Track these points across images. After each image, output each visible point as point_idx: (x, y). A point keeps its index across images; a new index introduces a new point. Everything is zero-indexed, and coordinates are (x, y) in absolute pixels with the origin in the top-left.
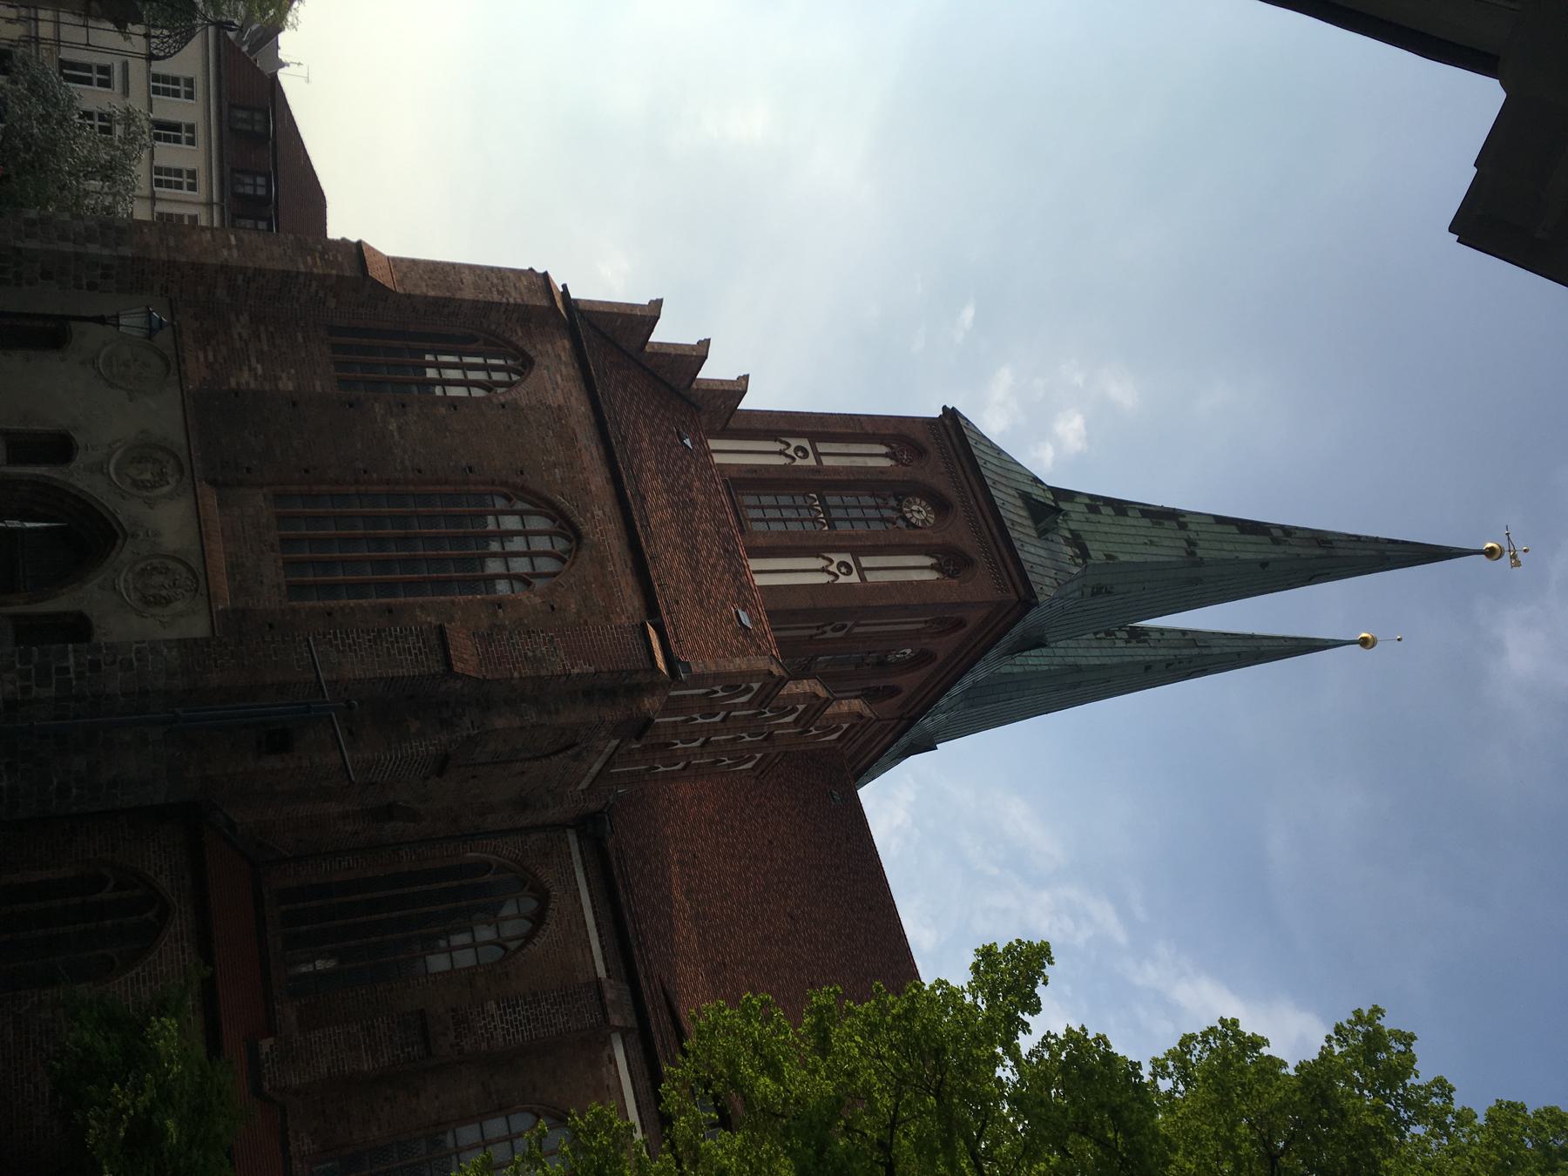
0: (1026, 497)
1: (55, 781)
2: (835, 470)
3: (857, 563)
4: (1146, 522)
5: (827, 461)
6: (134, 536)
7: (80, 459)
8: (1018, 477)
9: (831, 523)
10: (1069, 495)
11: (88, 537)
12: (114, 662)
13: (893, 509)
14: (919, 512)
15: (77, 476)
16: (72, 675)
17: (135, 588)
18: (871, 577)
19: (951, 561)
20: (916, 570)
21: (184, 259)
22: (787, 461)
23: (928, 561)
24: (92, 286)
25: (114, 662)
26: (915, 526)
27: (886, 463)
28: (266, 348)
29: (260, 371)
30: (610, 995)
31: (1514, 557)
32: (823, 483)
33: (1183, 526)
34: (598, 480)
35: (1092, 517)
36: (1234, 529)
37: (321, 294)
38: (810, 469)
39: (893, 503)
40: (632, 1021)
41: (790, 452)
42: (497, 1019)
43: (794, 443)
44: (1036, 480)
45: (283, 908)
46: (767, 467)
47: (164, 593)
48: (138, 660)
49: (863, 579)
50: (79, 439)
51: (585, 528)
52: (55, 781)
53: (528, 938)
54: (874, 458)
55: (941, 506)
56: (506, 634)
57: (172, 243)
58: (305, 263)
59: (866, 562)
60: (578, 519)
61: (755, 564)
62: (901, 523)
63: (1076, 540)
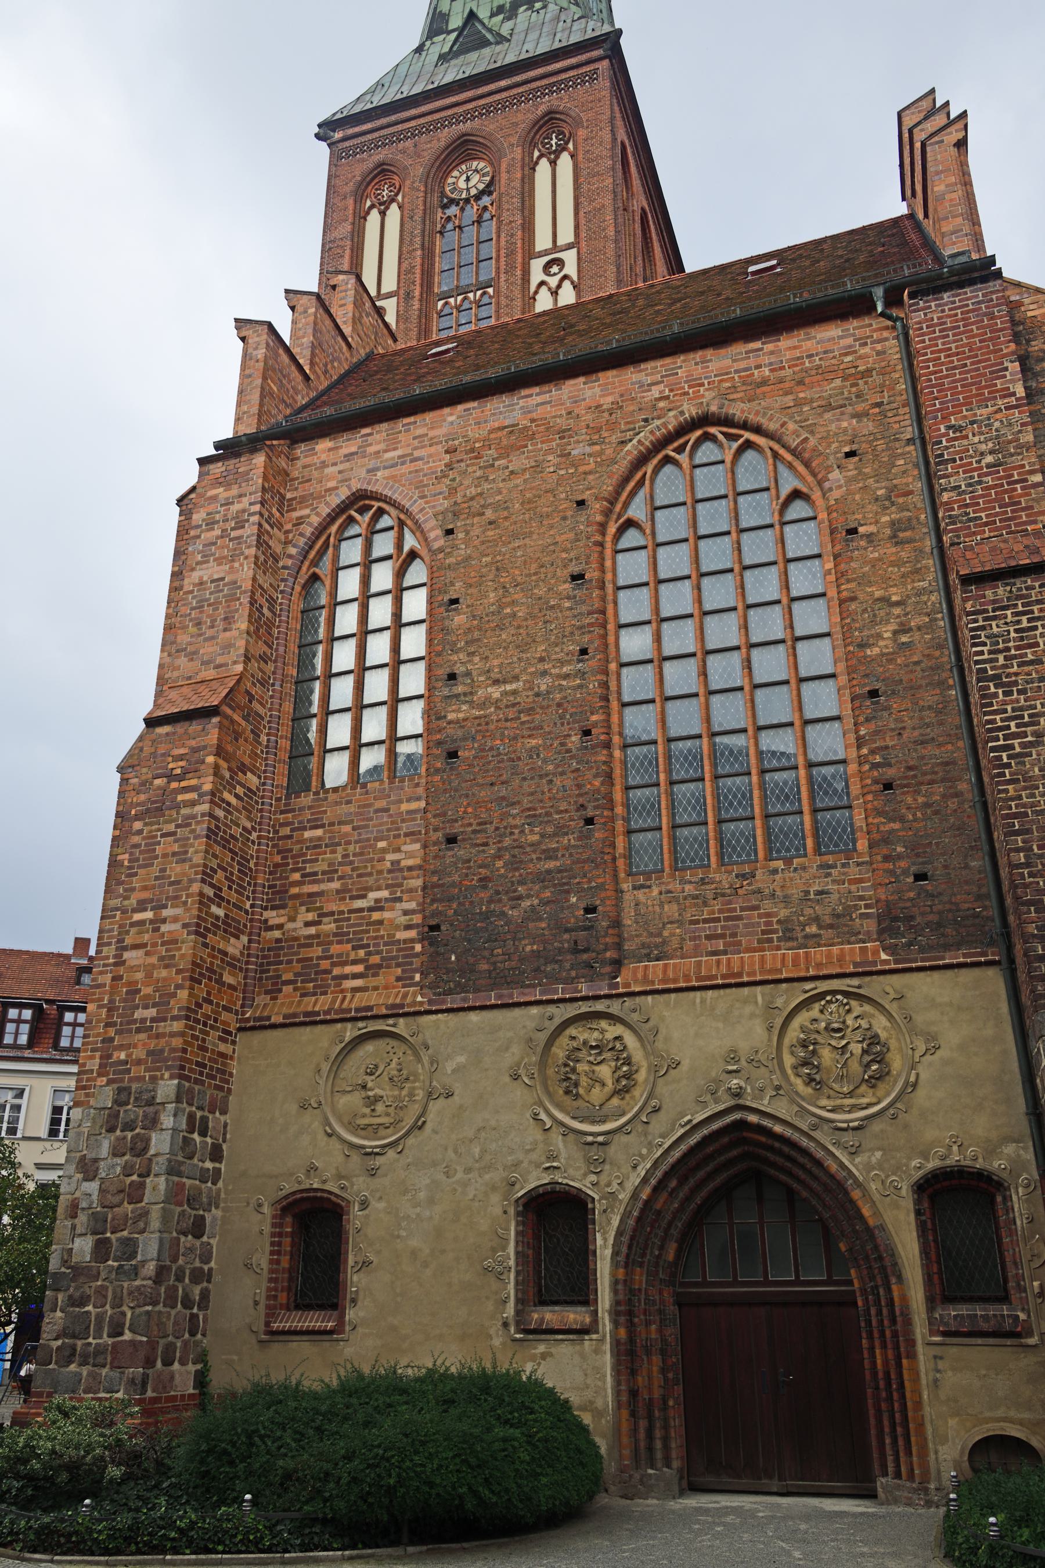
2: (402, 273)
3: (546, 253)
6: (738, 1094)
7: (581, 1182)
13: (462, 210)
15: (616, 1189)
17: (851, 1094)
18: (566, 235)
19: (549, 132)
21: (183, 994)
24: (216, 1154)
26: (491, 183)
28: (336, 885)
29: (385, 894)
37: (240, 790)
39: (453, 210)
50: (535, 1180)
57: (152, 1012)
58: (193, 803)
59: (542, 241)
62: (486, 200)
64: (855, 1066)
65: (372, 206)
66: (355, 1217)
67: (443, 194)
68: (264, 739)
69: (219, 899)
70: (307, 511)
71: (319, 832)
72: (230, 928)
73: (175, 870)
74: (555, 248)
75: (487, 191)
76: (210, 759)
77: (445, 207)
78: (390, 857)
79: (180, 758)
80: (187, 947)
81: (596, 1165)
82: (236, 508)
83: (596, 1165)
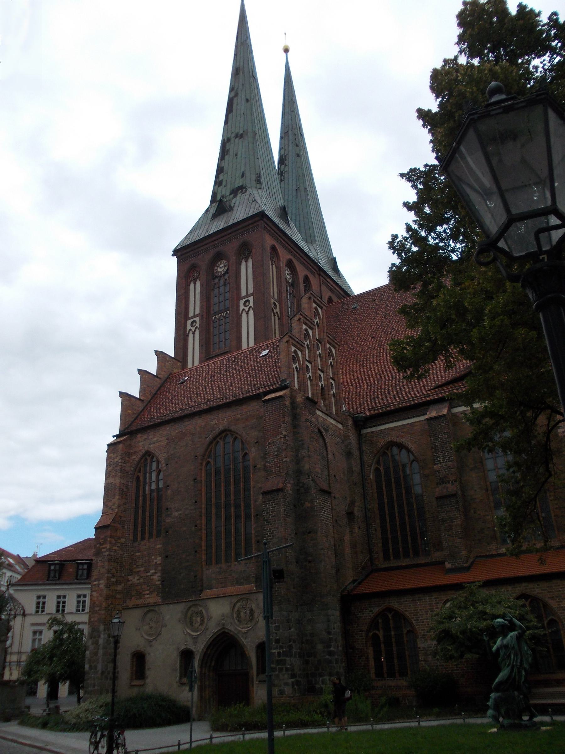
0: (215, 216)
1: (327, 657)
2: (201, 308)
4: (227, 157)
5: (198, 311)
7: (192, 648)
8: (204, 222)
9: (226, 310)
10: (214, 195)
11: (224, 645)
12: (276, 633)
13: (219, 280)
15: (199, 648)
16: (281, 651)
17: (246, 624)
18: (251, 291)
20: (246, 270)
21: (104, 604)
22: (197, 330)
25: (276, 633)
26: (227, 270)
27: (198, 284)
30: (434, 414)
32: (207, 313)
33: (229, 140)
34: (200, 422)
35: (224, 184)
36: (230, 115)
37: (119, 545)
38: (201, 320)
39: (216, 281)
40: (447, 404)
41: (193, 329)
42: (442, 464)
43: (189, 327)
44: (207, 211)
45: (392, 558)
46: (201, 340)
47: (248, 612)
48: (275, 623)
50: (183, 647)
51: (221, 428)
52: (327, 657)
53: (409, 451)
54: (195, 290)
56: (267, 464)
58: (105, 552)
59: (244, 293)
60: (217, 431)
61: (244, 346)
62: (226, 276)
64: (248, 617)
65: (191, 280)
66: (148, 658)
67: (213, 274)
68: (126, 527)
69: (113, 576)
70: (135, 457)
71: (139, 554)
72: (117, 583)
73: (103, 570)
74: (248, 295)
75: (226, 273)
76: (109, 539)
77: (214, 279)
78: (155, 561)
79: (102, 539)
80: (105, 592)
81: (195, 643)
82: (116, 460)
83: (195, 643)
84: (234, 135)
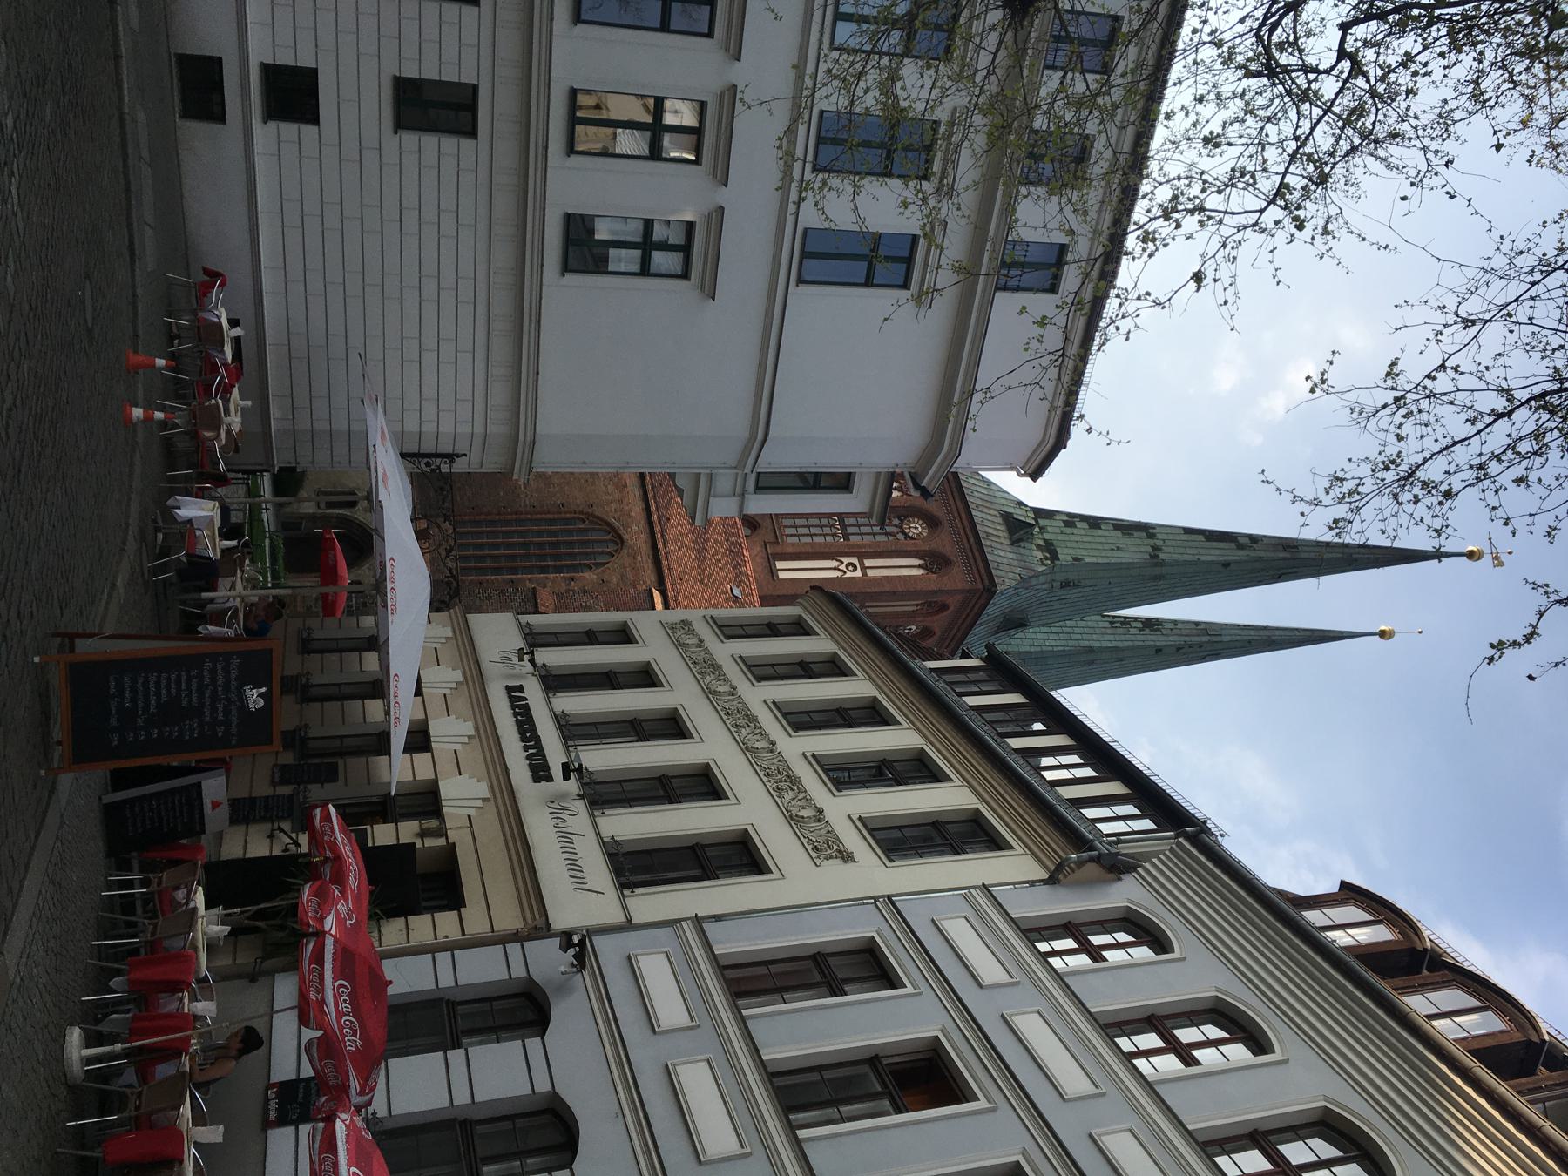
0: (1008, 518)
4: (1119, 533)
9: (846, 536)
10: (1049, 514)
14: (916, 528)
19: (935, 561)
20: (907, 568)
23: (917, 562)
31: (1496, 558)
33: (1152, 536)
34: (637, 509)
35: (1068, 530)
36: (1201, 538)
39: (896, 521)
44: (1021, 504)
49: (864, 574)
51: (626, 537)
55: (932, 522)
60: (622, 532)
61: (780, 565)
62: (900, 536)
63: (1050, 549)
75: (906, 536)
84: (1159, 543)
